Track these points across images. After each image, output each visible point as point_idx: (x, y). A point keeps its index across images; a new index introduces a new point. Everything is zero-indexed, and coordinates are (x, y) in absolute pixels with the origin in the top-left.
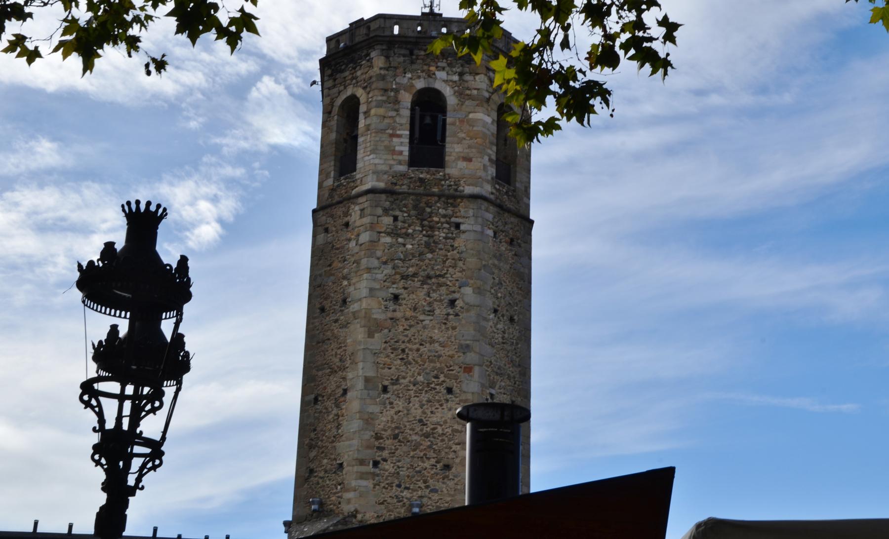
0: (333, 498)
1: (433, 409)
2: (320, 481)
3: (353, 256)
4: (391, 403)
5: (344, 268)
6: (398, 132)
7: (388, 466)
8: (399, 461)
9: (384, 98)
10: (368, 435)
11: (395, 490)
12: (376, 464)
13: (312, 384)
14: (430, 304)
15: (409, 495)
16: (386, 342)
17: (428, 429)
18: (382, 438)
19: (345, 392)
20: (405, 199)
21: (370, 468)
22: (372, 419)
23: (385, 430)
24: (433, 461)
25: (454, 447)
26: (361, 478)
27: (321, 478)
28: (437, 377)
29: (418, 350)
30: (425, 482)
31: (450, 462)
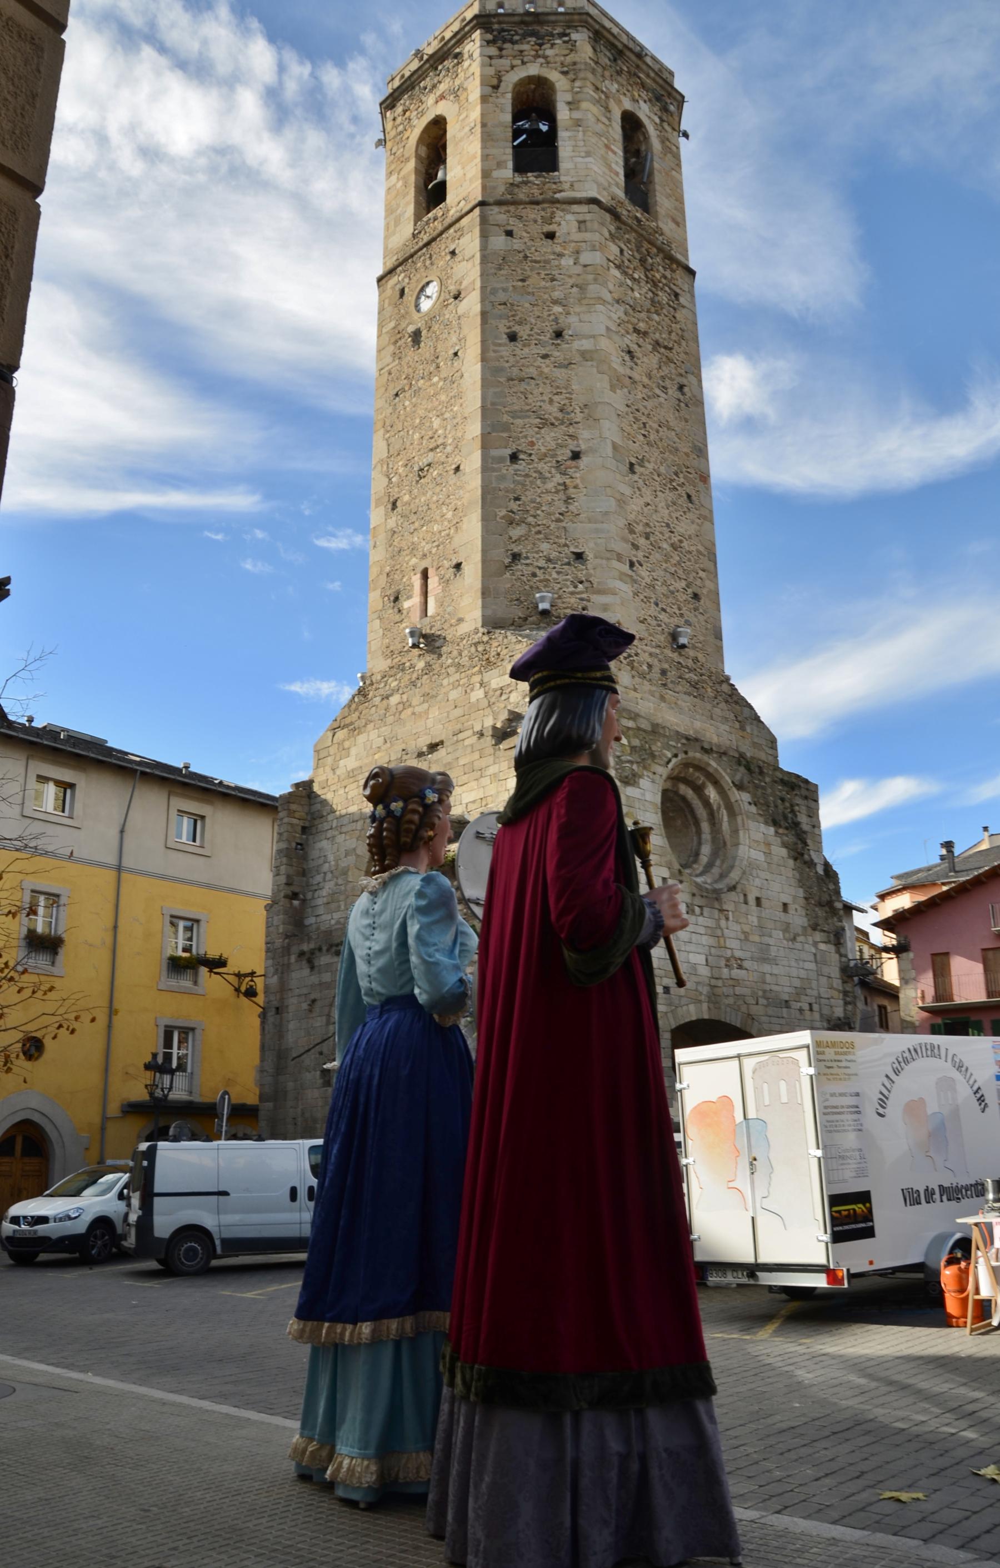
0: (573, 600)
1: (678, 514)
2: (538, 572)
3: (570, 276)
4: (638, 488)
5: (553, 289)
6: (613, 147)
7: (643, 572)
8: (654, 571)
9: (597, 97)
10: (622, 523)
11: (653, 610)
12: (632, 564)
13: (505, 435)
14: (663, 378)
15: (666, 620)
16: (627, 406)
17: (676, 539)
18: (635, 533)
19: (576, 456)
20: (628, 232)
21: (625, 568)
22: (624, 502)
23: (638, 524)
24: (683, 584)
25: (702, 574)
26: (621, 580)
27: (540, 568)
28: (676, 474)
29: (658, 432)
30: (680, 609)
31: (698, 591)
